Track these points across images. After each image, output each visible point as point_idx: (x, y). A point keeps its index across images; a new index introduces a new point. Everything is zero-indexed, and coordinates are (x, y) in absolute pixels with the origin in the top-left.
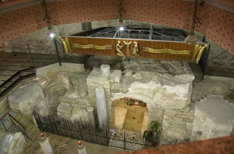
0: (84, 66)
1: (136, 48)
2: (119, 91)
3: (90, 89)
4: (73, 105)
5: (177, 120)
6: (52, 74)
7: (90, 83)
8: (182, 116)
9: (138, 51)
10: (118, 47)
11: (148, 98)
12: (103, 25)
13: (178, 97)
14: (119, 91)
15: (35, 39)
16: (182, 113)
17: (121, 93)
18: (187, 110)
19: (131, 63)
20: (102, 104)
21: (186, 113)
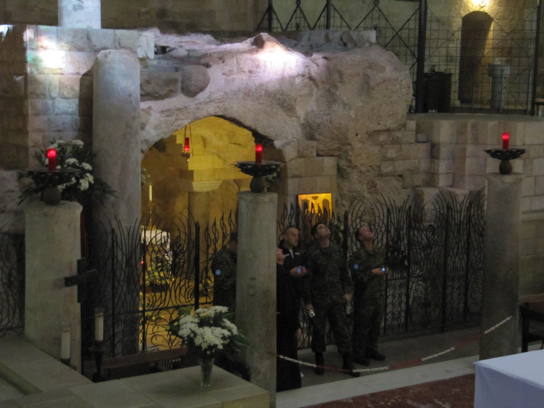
2: (172, 87)
8: (401, 166)
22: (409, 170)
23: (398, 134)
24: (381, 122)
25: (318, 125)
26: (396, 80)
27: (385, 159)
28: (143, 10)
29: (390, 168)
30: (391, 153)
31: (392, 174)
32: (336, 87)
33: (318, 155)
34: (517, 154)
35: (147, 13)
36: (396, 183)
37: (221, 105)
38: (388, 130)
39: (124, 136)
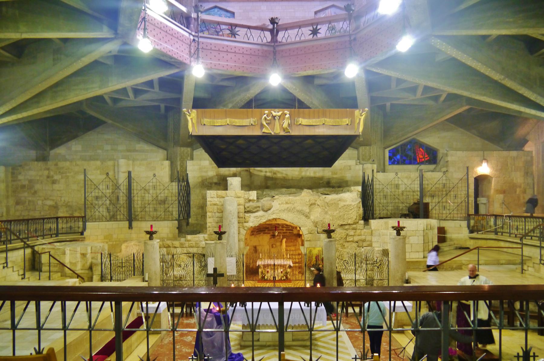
0: (177, 226)
1: (288, 118)
2: (258, 209)
3: (211, 210)
4: (173, 251)
5: (349, 247)
6: (113, 241)
7: (212, 198)
8: (356, 238)
9: (290, 123)
10: (265, 119)
11: (302, 216)
12: (207, 172)
13: (344, 202)
14: (258, 209)
15: (69, 202)
16: (355, 232)
17: (261, 213)
18: (360, 224)
19: (265, 195)
20: (234, 223)
21: (360, 231)
22: (361, 240)
23: (354, 226)
24: (345, 221)
25: (317, 222)
26: (351, 205)
27: (347, 235)
28: (321, 182)
29: (352, 239)
30: (352, 233)
31: (352, 241)
32: (326, 208)
33: (318, 233)
34: (333, 231)
35: (322, 183)
36: (355, 245)
37: (278, 215)
38: (349, 224)
39: (229, 224)
